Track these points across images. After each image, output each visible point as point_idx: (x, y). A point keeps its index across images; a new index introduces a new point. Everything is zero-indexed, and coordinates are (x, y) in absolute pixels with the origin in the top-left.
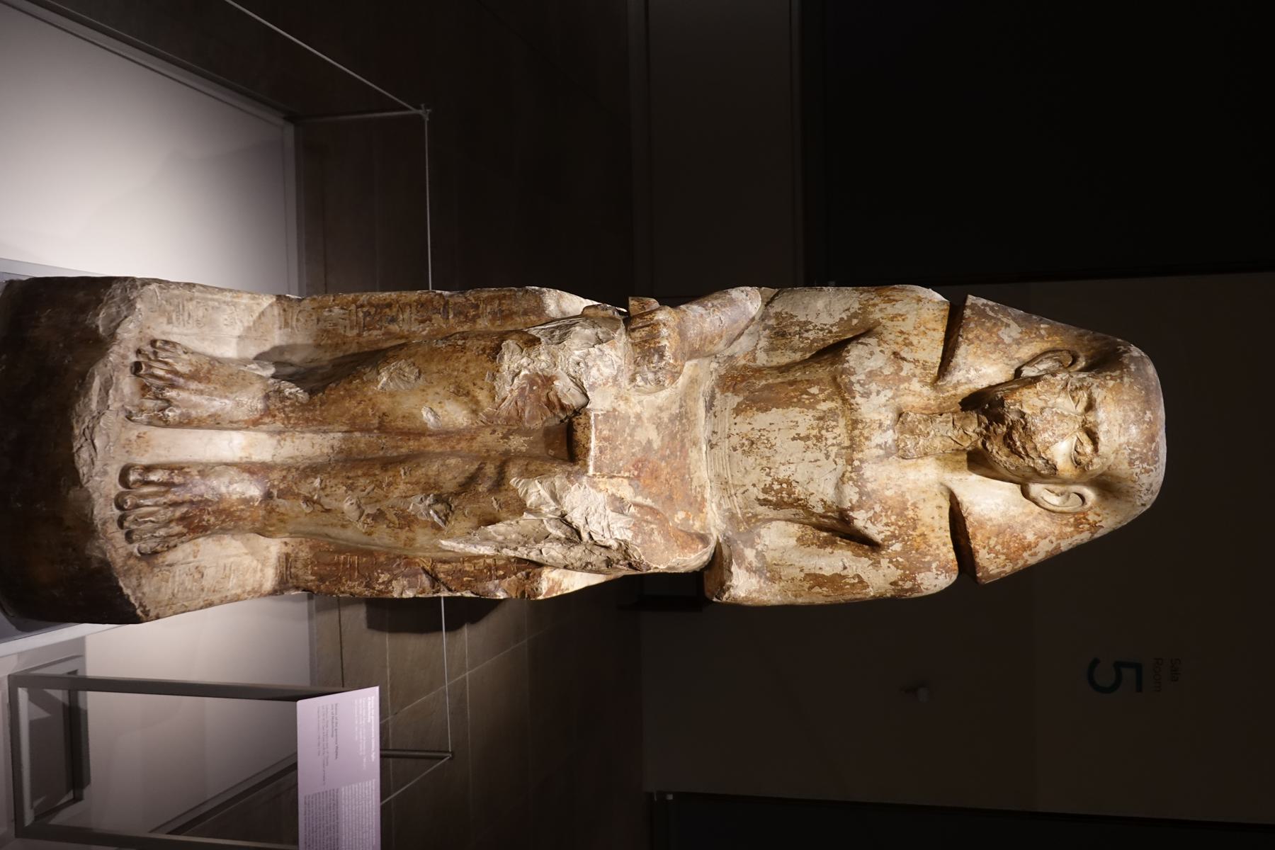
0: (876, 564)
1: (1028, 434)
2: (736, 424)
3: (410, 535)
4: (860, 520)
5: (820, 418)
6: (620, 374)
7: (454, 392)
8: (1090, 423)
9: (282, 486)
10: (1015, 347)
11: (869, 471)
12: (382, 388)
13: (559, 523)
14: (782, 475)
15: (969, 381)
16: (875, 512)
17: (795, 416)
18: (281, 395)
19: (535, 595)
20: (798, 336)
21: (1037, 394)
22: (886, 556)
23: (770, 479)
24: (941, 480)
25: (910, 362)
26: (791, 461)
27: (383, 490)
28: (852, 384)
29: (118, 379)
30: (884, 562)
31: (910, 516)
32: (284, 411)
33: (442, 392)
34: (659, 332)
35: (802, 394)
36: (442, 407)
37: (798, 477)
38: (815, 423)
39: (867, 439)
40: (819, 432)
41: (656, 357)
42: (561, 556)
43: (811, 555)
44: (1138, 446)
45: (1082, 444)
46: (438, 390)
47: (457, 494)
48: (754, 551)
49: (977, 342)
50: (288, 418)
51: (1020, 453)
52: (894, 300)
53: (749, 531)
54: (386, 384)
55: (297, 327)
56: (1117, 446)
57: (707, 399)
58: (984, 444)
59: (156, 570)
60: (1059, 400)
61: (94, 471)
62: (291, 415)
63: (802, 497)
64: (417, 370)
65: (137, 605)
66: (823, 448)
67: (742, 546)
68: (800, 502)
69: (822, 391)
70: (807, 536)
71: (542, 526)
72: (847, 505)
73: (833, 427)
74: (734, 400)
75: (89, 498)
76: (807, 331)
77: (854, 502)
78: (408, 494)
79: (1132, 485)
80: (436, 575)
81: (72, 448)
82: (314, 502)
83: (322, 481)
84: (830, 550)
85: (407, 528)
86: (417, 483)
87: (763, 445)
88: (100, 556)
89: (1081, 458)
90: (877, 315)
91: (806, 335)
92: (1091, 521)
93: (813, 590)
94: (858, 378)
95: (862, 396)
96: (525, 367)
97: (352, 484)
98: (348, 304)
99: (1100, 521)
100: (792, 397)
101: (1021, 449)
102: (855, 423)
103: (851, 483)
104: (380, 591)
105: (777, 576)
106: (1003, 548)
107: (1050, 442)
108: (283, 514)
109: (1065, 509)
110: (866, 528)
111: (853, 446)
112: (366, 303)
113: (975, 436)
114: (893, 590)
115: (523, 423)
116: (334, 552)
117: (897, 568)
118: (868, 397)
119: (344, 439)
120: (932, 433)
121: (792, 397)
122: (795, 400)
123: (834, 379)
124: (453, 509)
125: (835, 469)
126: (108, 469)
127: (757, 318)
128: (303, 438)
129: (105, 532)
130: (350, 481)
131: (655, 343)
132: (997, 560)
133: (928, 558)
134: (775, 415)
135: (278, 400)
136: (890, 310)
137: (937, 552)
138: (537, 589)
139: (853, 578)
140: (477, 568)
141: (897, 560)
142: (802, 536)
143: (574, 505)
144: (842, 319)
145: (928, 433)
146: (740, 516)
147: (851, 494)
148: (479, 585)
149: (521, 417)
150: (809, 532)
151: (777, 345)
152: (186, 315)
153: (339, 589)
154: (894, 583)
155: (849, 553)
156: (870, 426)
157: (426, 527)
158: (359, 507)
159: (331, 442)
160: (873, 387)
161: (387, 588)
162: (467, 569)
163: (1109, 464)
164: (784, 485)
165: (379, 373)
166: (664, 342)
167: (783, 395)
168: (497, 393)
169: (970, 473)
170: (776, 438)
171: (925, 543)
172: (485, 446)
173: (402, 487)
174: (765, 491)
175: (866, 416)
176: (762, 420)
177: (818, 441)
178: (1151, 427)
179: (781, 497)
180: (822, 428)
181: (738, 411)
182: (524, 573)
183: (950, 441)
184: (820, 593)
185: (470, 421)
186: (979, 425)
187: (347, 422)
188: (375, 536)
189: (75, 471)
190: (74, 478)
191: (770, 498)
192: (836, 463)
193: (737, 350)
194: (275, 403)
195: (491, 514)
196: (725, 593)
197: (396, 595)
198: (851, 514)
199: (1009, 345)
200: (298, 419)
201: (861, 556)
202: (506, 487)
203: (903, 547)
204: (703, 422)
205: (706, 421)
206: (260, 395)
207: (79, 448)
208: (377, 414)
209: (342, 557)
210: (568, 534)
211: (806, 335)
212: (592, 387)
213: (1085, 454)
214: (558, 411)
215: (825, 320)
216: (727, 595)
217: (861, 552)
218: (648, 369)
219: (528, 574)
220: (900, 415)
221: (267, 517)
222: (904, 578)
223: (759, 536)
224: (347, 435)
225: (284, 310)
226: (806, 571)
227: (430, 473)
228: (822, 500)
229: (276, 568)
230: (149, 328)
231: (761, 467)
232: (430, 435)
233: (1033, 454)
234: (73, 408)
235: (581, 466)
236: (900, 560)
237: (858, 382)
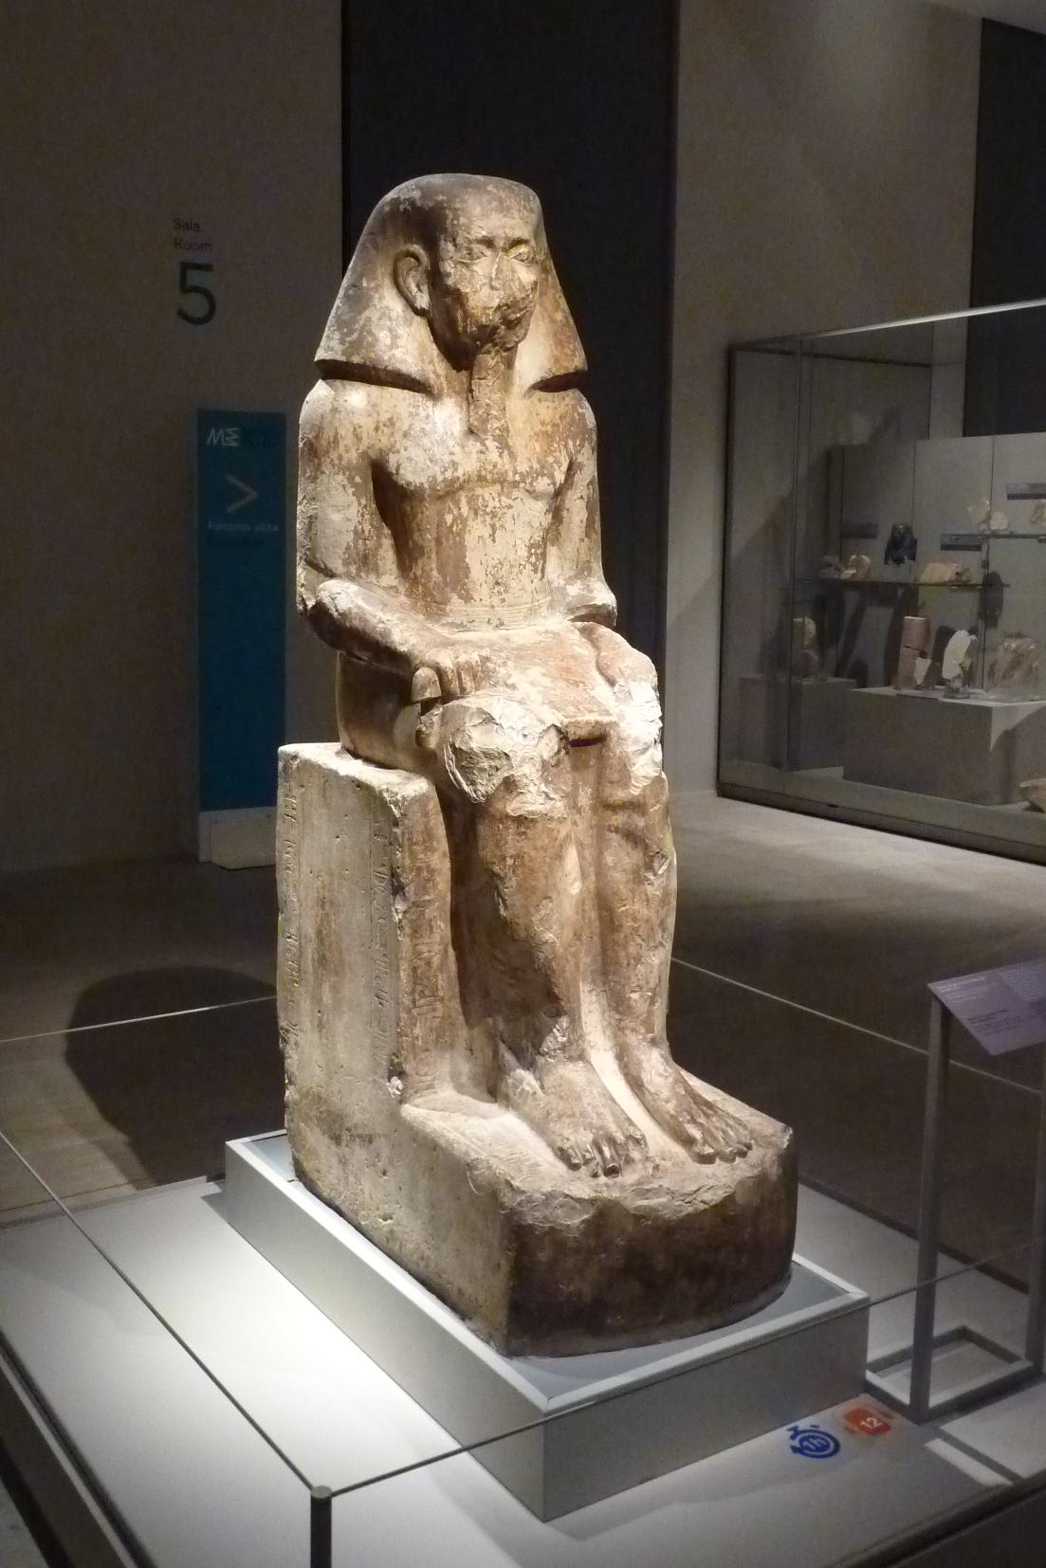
5: (476, 514)
9: (643, 1031)
14: (523, 552)
20: (367, 542)
21: (474, 292)
28: (445, 480)
39: (495, 466)
40: (488, 514)
41: (489, 664)
43: (569, 530)
44: (520, 202)
52: (335, 437)
56: (521, 222)
75: (741, 1183)
76: (363, 531)
78: (644, 898)
81: (705, 1210)
82: (654, 994)
83: (633, 991)
84: (565, 512)
86: (633, 891)
90: (353, 456)
91: (367, 533)
94: (439, 473)
95: (456, 470)
97: (634, 959)
100: (455, 542)
102: (481, 479)
103: (534, 484)
105: (587, 565)
111: (501, 480)
121: (455, 542)
122: (457, 539)
123: (440, 498)
130: (632, 961)
134: (472, 559)
144: (354, 494)
145: (488, 405)
155: (569, 493)
164: (533, 551)
165: (547, 942)
167: (452, 552)
173: (636, 907)
176: (477, 573)
180: (485, 511)
181: (467, 598)
192: (516, 498)
198: (558, 485)
202: (641, 798)
211: (367, 533)
215: (353, 512)
225: (416, 1092)
237: (443, 473)
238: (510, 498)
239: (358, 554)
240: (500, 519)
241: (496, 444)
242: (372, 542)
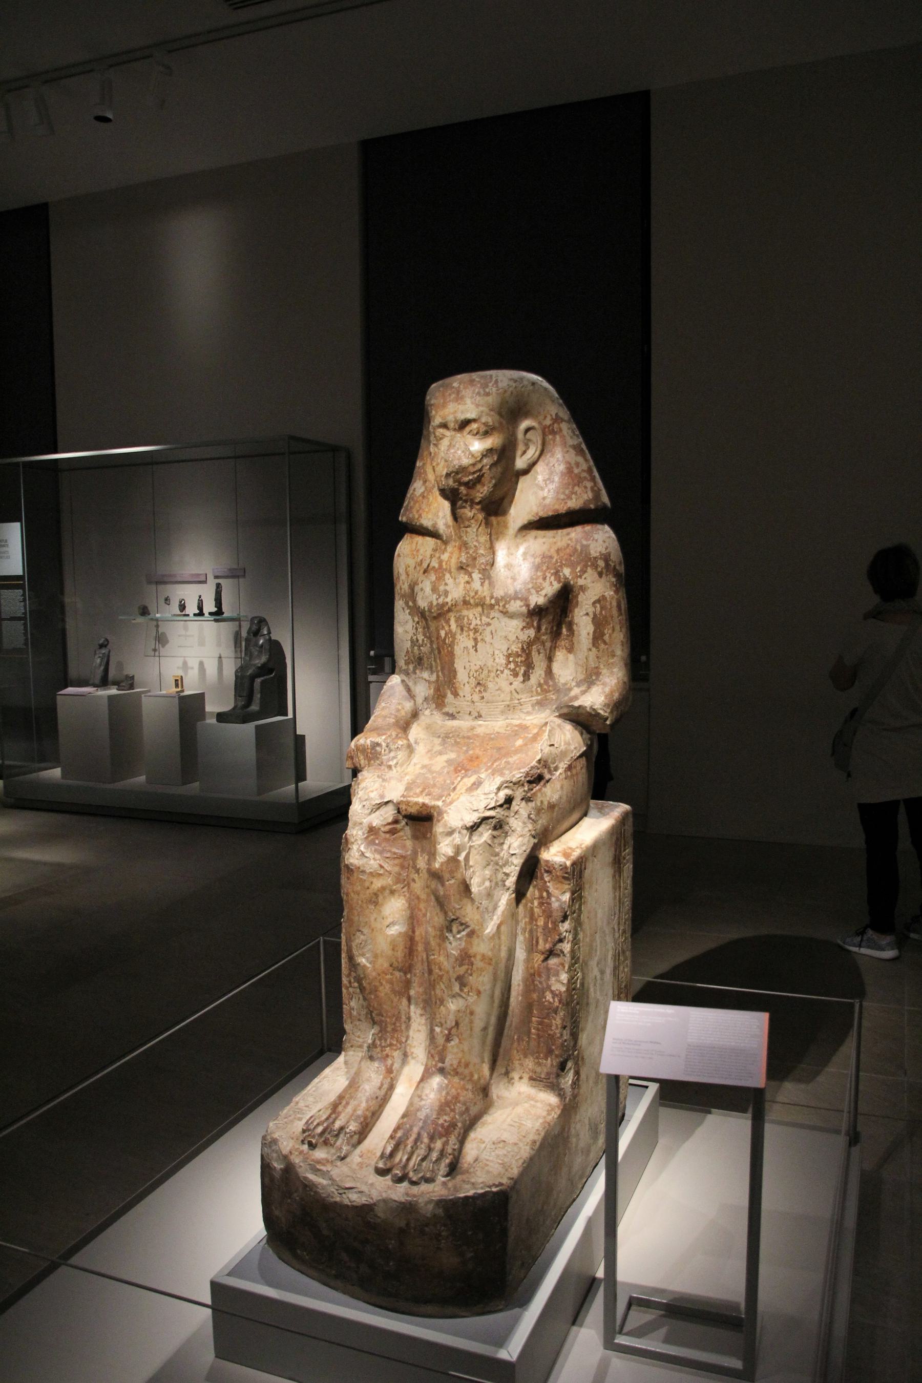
0: (583, 589)
1: (462, 470)
2: (464, 696)
3: (479, 957)
4: (538, 600)
5: (462, 630)
6: (383, 777)
7: (375, 906)
8: (455, 425)
9: (437, 1059)
10: (427, 484)
11: (499, 593)
12: (370, 963)
13: (476, 833)
14: (503, 661)
15: (444, 517)
16: (532, 587)
17: (460, 649)
18: (371, 1046)
19: (566, 867)
20: (421, 648)
23: (506, 671)
24: (513, 537)
25: (430, 562)
26: (492, 653)
27: (443, 975)
28: (438, 604)
29: (313, 1160)
30: (581, 582)
31: (540, 561)
32: (384, 1047)
33: (375, 915)
34: (361, 745)
35: (445, 644)
36: (387, 918)
37: (505, 648)
38: (465, 633)
39: (476, 593)
40: (471, 630)
41: (378, 749)
42: (520, 839)
43: (579, 642)
44: (474, 390)
45: (471, 431)
46: (372, 919)
47: (446, 913)
48: (575, 688)
49: (421, 511)
50: (391, 1045)
51: (478, 476)
53: (558, 691)
54: (367, 959)
55: (363, 1039)
57: (447, 718)
58: (478, 504)
59: (472, 1170)
60: (442, 449)
61: (367, 1192)
62: (388, 1042)
63: (520, 645)
64: (358, 933)
65: (488, 1189)
66: (483, 628)
67: (566, 698)
68: (525, 648)
69: (443, 628)
70: (567, 645)
71: (476, 846)
73: (468, 619)
74: (450, 696)
75: (385, 1201)
76: (417, 641)
77: (522, 604)
78: (446, 953)
79: (509, 393)
80: (547, 951)
81: (347, 1206)
82: (450, 1033)
83: (437, 1026)
85: (472, 959)
86: (439, 945)
87: (481, 676)
88: (432, 1205)
89: (481, 431)
90: (406, 587)
91: (420, 642)
95: (447, 597)
96: (359, 847)
97: (440, 1000)
98: (349, 994)
99: (551, 415)
100: (448, 651)
101: (475, 476)
102: (466, 603)
103: (507, 606)
104: (560, 1002)
105: (595, 671)
106: (568, 488)
107: (469, 454)
108: (460, 1062)
109: (540, 442)
110: (546, 595)
111: (481, 604)
112: (348, 979)
113: (474, 511)
114: (607, 575)
115: (408, 855)
116: (529, 1037)
117: (585, 572)
118: (448, 592)
119: (416, 1004)
120: (475, 543)
121: (448, 651)
122: (450, 649)
123: (435, 618)
124: (455, 918)
125: (498, 618)
126: (370, 1182)
127: (405, 678)
128: (413, 1038)
129: (414, 1196)
130: (438, 1001)
131: (368, 749)
132: (578, 493)
133: (579, 548)
134: (459, 665)
135: (374, 1050)
136: (403, 577)
137: (574, 540)
138: (561, 866)
139: (595, 607)
140: (541, 915)
141: (579, 572)
142: (566, 649)
143: (460, 818)
144: (410, 614)
145: (475, 546)
146: (539, 698)
147: (516, 606)
148: (555, 914)
149: (402, 856)
150: (563, 643)
151: (428, 664)
152: (305, 1108)
153: (558, 1038)
154: (600, 575)
155: (576, 610)
156: (468, 591)
157: (471, 943)
158: (454, 996)
159: (418, 1016)
160: (442, 588)
161: (557, 995)
162: (542, 923)
163: (488, 411)
164: (511, 659)
165: (359, 964)
166: (368, 742)
168: (375, 871)
169: (508, 515)
170: (475, 665)
171: (565, 549)
172: (424, 889)
173: (442, 959)
174: (516, 675)
175: (461, 594)
176: (462, 676)
177: (478, 632)
178: (464, 383)
179: (521, 662)
180: (469, 628)
181: (456, 694)
182: (545, 875)
184: (610, 636)
185: (403, 897)
186: (465, 507)
187: (398, 997)
188: (482, 989)
189: (364, 1206)
190: (366, 1210)
191: (522, 671)
192: (493, 618)
193: (423, 694)
194: (376, 1052)
195: (459, 886)
196: (599, 713)
197: (564, 989)
198: (532, 606)
199: (426, 488)
200: (392, 1038)
201: (578, 601)
202: (440, 871)
203: (567, 566)
204: (462, 722)
205: (462, 720)
206: (369, 1062)
207: (349, 1200)
208: (391, 971)
209: (533, 1030)
210: (488, 827)
211: (420, 642)
212: (382, 796)
213: (478, 428)
214: (398, 826)
215: (410, 626)
216: (601, 712)
217: (574, 601)
218: (385, 755)
219: (547, 872)
220: (462, 568)
221: (461, 1077)
222: (595, 566)
223: (566, 684)
224: (413, 1001)
225: (352, 1046)
226: (591, 646)
227: (433, 934)
228: (522, 629)
229: (540, 1090)
230: (294, 1133)
231: (496, 678)
232: (414, 932)
233: (479, 466)
234: (324, 1199)
235: (435, 810)
236: (579, 569)
237: (437, 599)
238: (489, 618)
239: (414, 656)
240: (481, 634)
241: (480, 576)
242: (426, 648)
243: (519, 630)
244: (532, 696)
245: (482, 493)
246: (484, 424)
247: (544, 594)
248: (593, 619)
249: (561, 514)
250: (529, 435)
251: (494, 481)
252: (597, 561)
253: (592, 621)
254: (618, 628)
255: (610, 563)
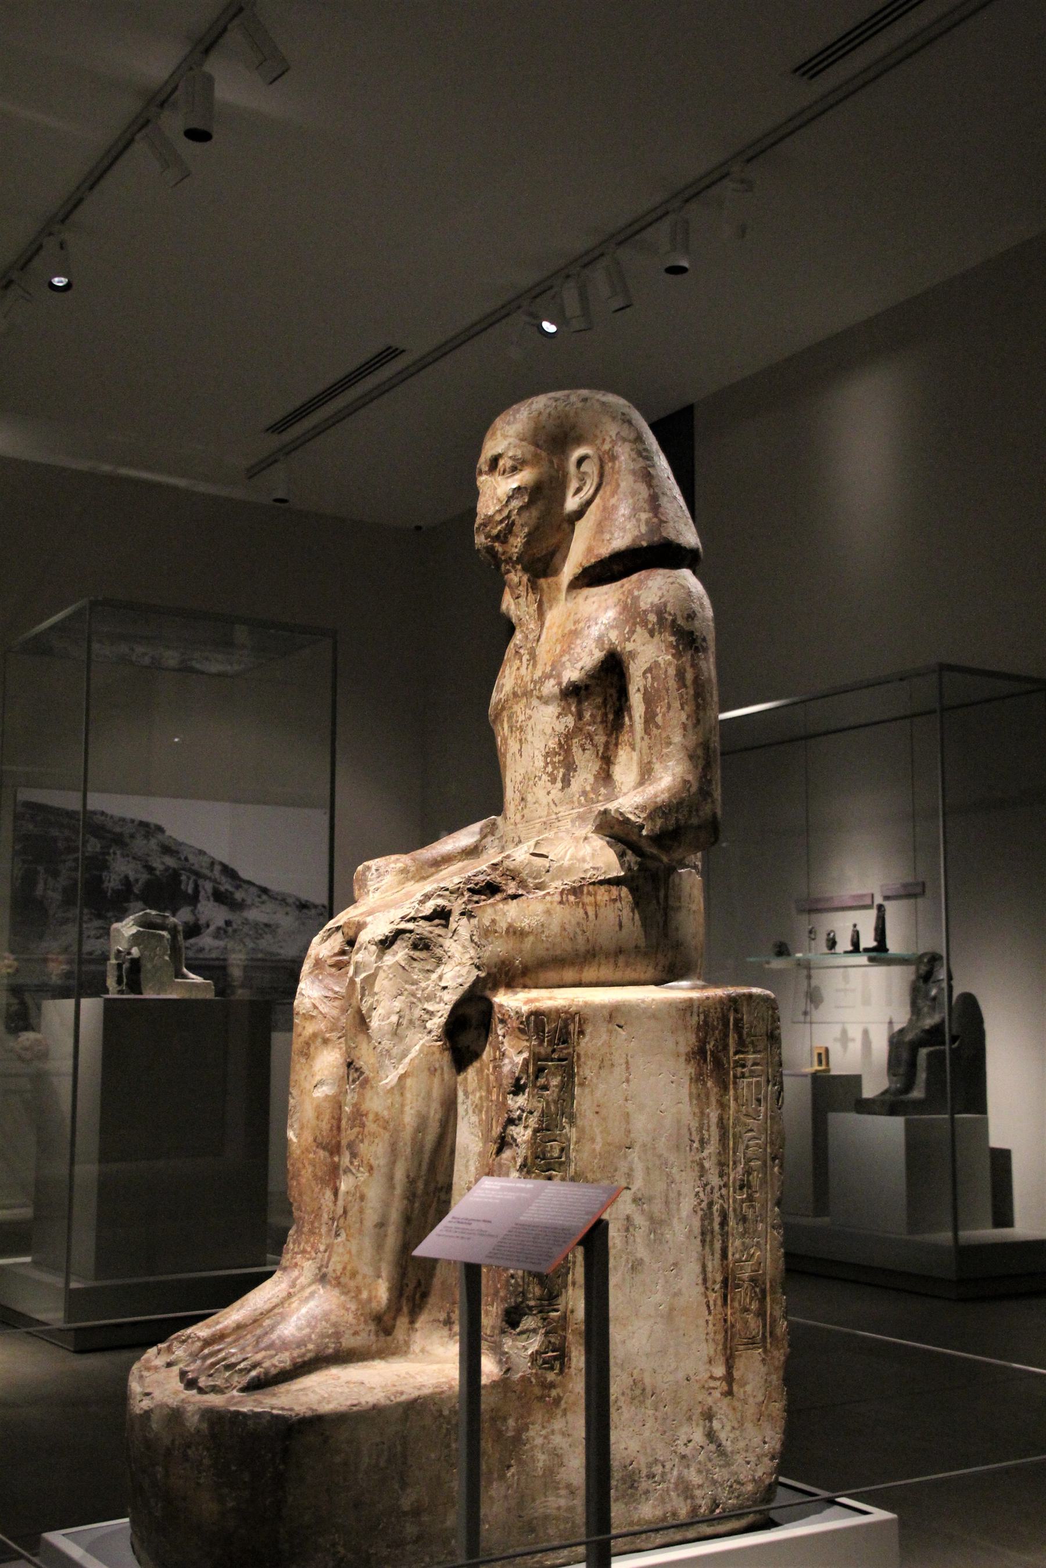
0: (632, 655)
7: (307, 1059)
22: (623, 645)
30: (629, 646)
33: (305, 1072)
50: (304, 1252)
51: (507, 525)
62: (302, 1247)
63: (557, 740)
72: (556, 690)
85: (364, 1118)
92: (610, 446)
93: (660, 723)
99: (611, 437)
101: (504, 525)
108: (344, 1268)
109: (596, 473)
110: (582, 668)
114: (660, 633)
139: (646, 678)
141: (628, 633)
146: (581, 810)
150: (626, 738)
154: (652, 634)
157: (363, 1095)
163: (518, 442)
164: (549, 760)
168: (308, 1012)
179: (559, 762)
183: (529, 598)
184: (664, 715)
187: (320, 1186)
188: (374, 1163)
191: (561, 775)
195: (354, 1017)
196: (628, 819)
198: (564, 684)
200: (307, 1242)
222: (645, 623)
228: (558, 717)
233: (505, 513)
236: (627, 629)
243: (555, 718)
244: (573, 809)
245: (516, 547)
246: (510, 457)
247: (580, 667)
248: (644, 694)
249: (605, 558)
250: (584, 467)
251: (526, 530)
252: (646, 616)
253: (643, 698)
254: (677, 704)
255: (666, 616)
